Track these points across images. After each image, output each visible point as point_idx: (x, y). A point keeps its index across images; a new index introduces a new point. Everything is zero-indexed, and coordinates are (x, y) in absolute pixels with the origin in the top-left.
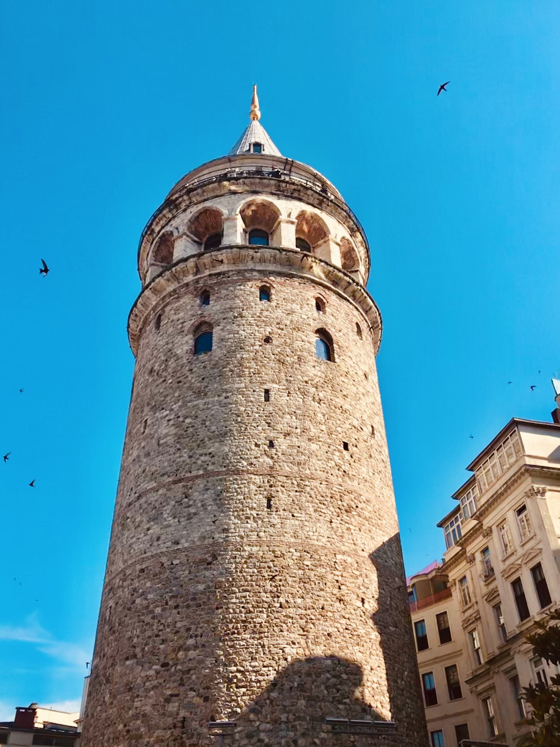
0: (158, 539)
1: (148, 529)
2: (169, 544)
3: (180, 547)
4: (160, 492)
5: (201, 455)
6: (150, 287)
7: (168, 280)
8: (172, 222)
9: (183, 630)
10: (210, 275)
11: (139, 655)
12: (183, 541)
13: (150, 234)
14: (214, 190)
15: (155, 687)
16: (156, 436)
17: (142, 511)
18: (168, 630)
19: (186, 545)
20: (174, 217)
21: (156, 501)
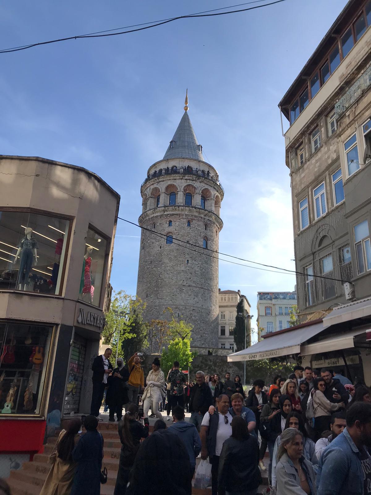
0: (198, 303)
1: (194, 298)
2: (201, 305)
3: (203, 307)
4: (197, 289)
5: (207, 283)
6: (189, 208)
7: (197, 211)
8: (194, 182)
9: (205, 329)
10: (208, 219)
11: (195, 332)
12: (204, 306)
13: (183, 176)
14: (211, 183)
15: (200, 341)
16: (194, 269)
17: (191, 291)
18: (202, 328)
19: (205, 307)
20: (196, 181)
21: (196, 291)
